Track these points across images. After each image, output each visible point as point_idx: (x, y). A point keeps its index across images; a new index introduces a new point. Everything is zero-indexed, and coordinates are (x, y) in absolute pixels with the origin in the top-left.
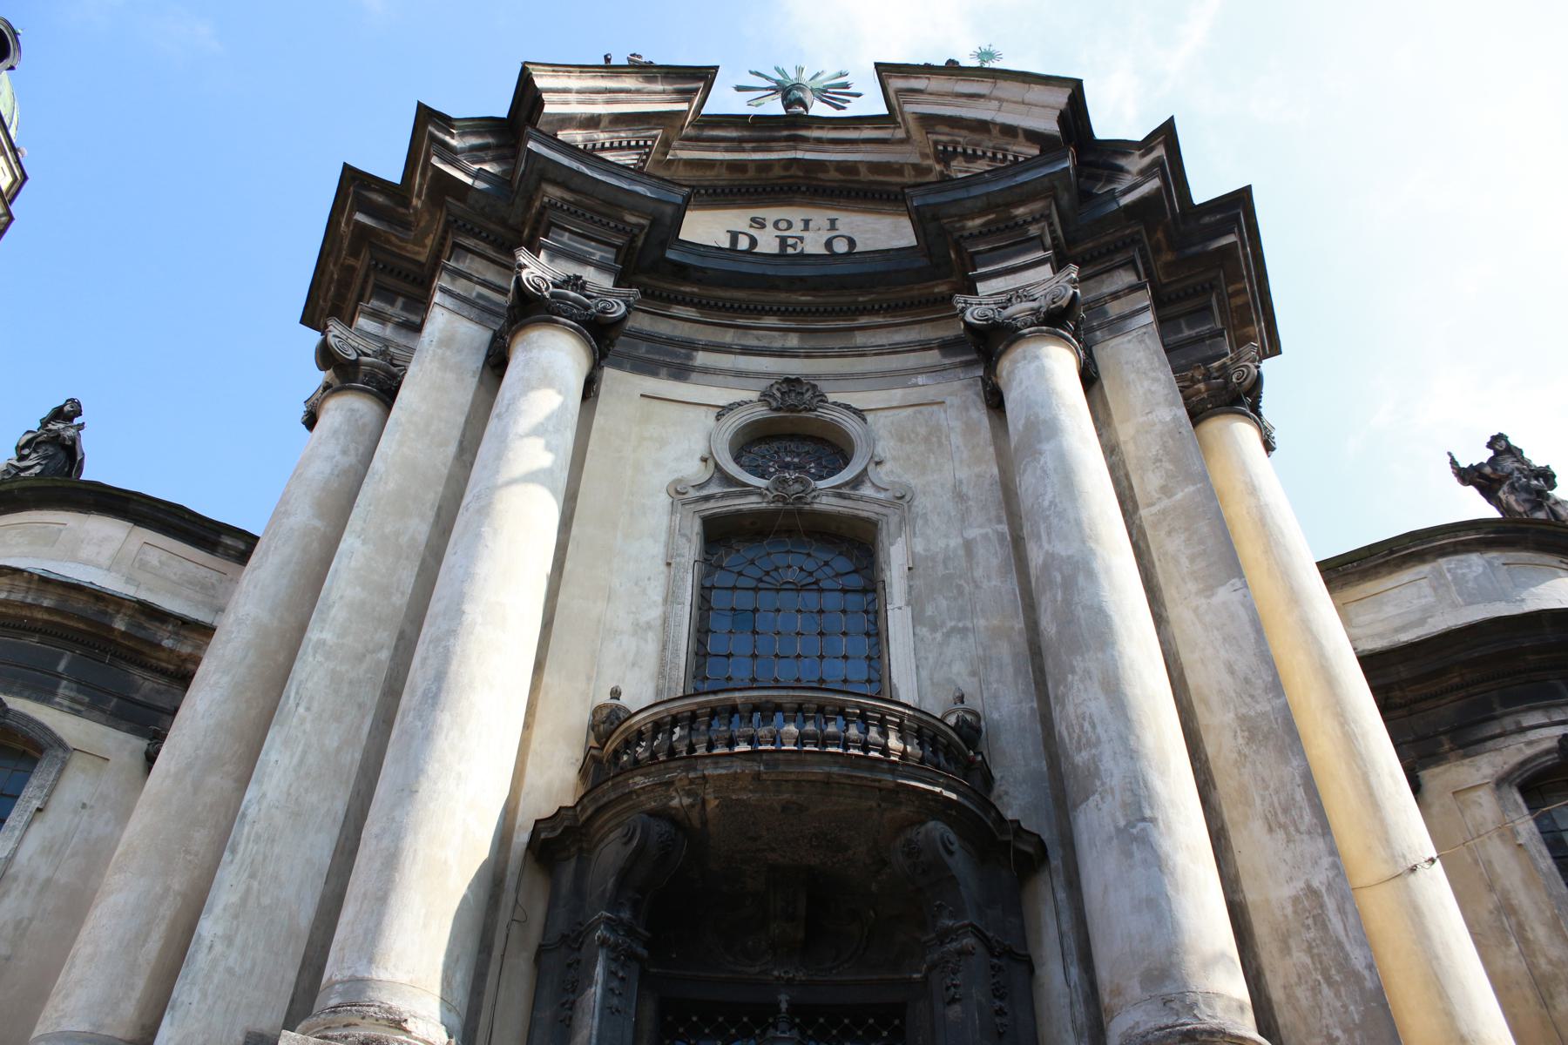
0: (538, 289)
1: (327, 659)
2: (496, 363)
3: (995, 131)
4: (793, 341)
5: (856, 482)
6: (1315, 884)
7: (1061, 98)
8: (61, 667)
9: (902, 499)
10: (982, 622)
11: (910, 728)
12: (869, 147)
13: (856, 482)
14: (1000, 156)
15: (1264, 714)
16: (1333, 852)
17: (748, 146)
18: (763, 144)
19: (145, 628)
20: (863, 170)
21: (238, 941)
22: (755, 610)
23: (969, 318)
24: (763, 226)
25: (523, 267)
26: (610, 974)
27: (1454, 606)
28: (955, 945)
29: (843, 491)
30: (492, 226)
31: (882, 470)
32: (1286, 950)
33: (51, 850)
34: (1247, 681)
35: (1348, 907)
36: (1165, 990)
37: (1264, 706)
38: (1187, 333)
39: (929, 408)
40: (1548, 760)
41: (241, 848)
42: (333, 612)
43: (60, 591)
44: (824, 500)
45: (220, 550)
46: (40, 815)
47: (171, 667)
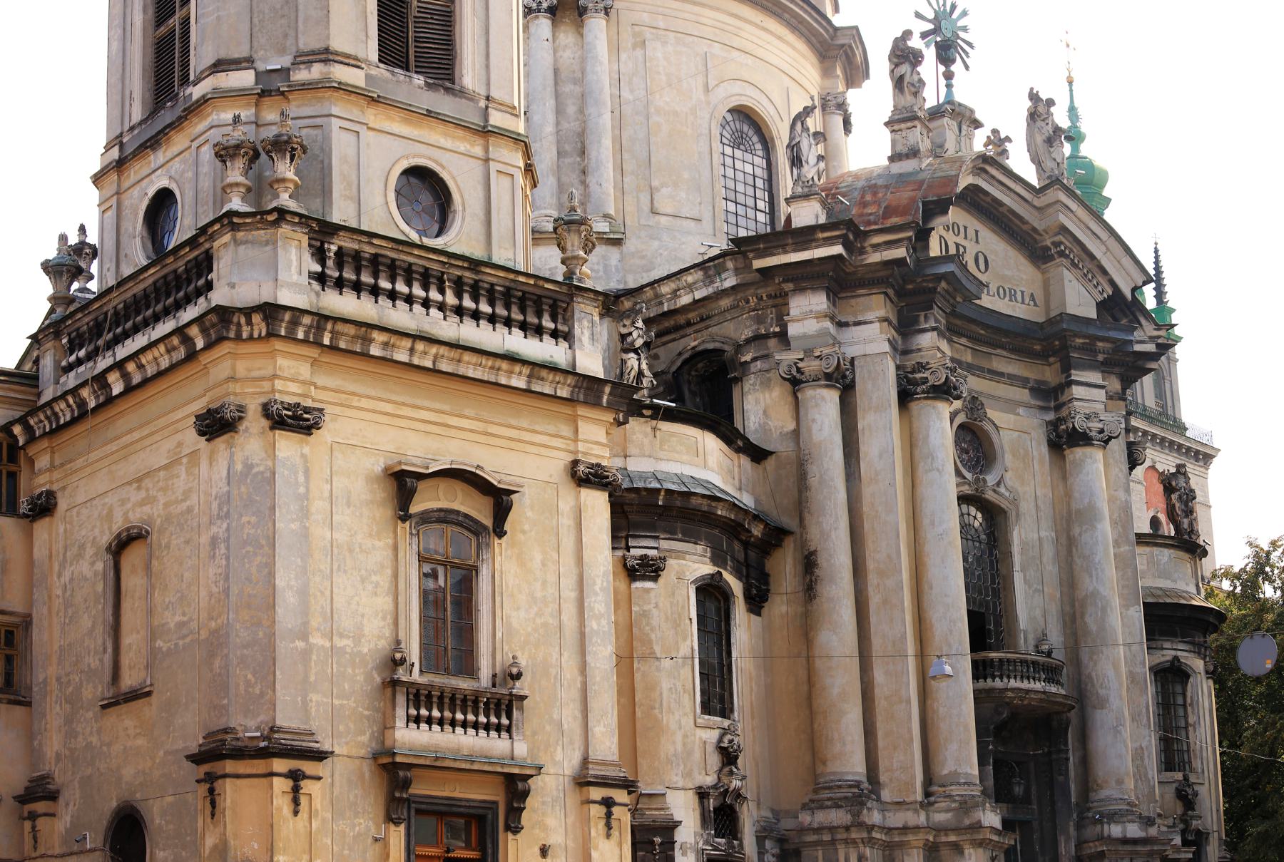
4: (968, 357)
5: (998, 484)
9: (1015, 501)
13: (998, 484)
27: (1154, 576)
40: (1167, 665)
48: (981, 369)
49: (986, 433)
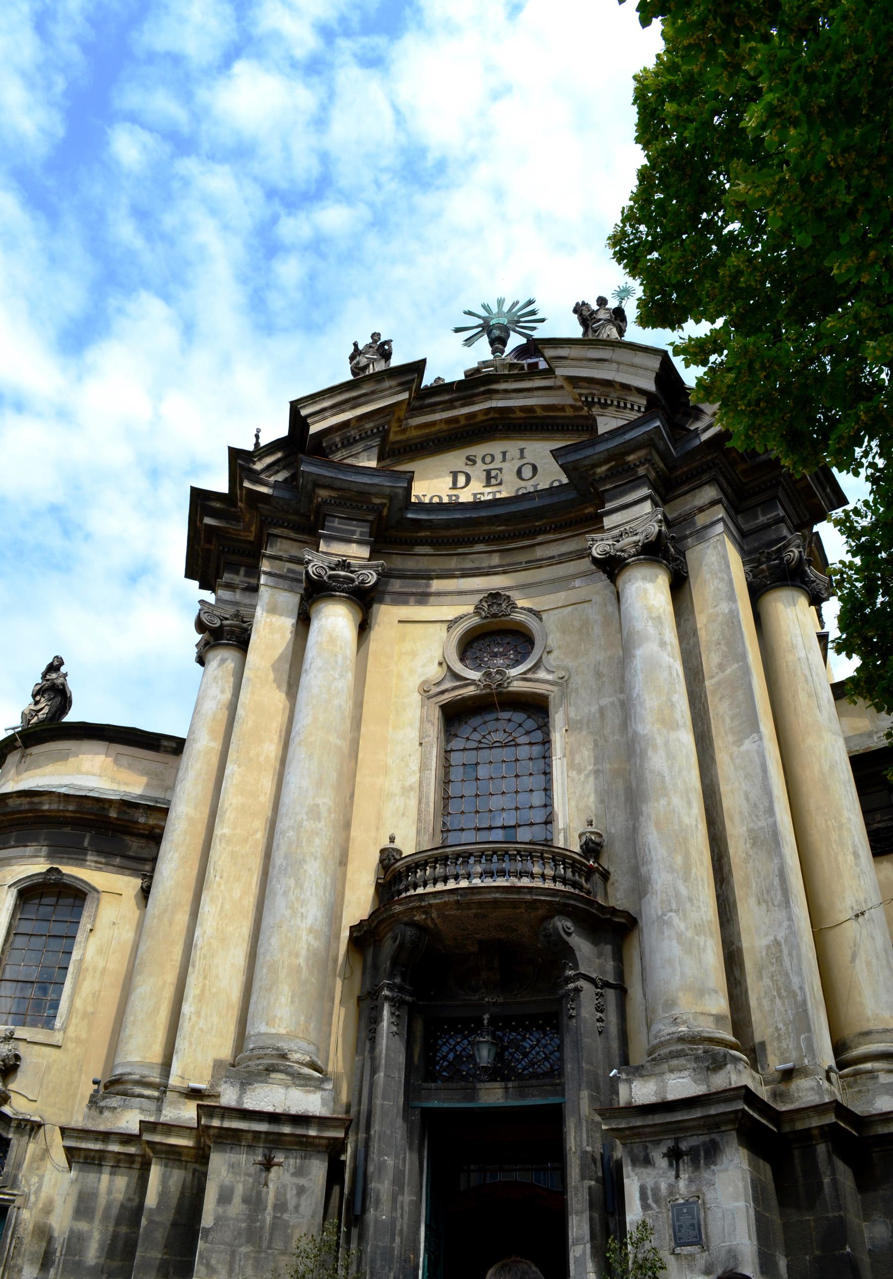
0: (320, 576)
1: (228, 845)
2: (304, 620)
3: (617, 387)
4: (495, 560)
5: (536, 667)
6: (779, 938)
7: (655, 363)
8: (86, 844)
10: (608, 766)
11: (548, 858)
12: (540, 393)
14: (622, 404)
15: (762, 828)
16: (790, 919)
17: (457, 404)
18: (468, 401)
19: (127, 813)
20: (539, 410)
21: (203, 1013)
22: (477, 764)
23: (595, 553)
24: (474, 462)
25: (308, 562)
26: (392, 1014)
28: (571, 986)
29: (529, 676)
30: (290, 517)
31: (552, 657)
32: (760, 977)
33: (100, 951)
34: (755, 805)
35: (794, 953)
36: (673, 1012)
37: (762, 823)
38: (762, 519)
39: (582, 605)
41: (197, 963)
42: (227, 814)
43: (76, 800)
44: (515, 683)
45: (162, 749)
46: (92, 934)
47: (146, 832)
48: (521, 563)
49: (521, 624)
